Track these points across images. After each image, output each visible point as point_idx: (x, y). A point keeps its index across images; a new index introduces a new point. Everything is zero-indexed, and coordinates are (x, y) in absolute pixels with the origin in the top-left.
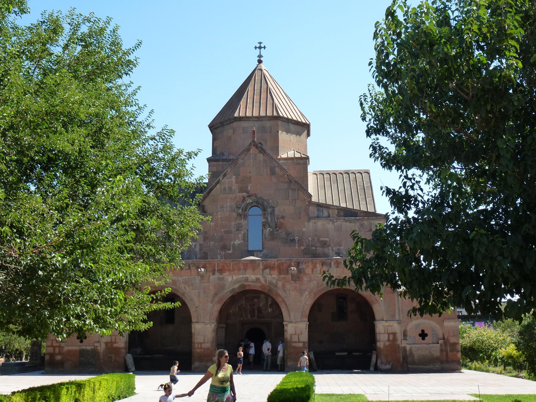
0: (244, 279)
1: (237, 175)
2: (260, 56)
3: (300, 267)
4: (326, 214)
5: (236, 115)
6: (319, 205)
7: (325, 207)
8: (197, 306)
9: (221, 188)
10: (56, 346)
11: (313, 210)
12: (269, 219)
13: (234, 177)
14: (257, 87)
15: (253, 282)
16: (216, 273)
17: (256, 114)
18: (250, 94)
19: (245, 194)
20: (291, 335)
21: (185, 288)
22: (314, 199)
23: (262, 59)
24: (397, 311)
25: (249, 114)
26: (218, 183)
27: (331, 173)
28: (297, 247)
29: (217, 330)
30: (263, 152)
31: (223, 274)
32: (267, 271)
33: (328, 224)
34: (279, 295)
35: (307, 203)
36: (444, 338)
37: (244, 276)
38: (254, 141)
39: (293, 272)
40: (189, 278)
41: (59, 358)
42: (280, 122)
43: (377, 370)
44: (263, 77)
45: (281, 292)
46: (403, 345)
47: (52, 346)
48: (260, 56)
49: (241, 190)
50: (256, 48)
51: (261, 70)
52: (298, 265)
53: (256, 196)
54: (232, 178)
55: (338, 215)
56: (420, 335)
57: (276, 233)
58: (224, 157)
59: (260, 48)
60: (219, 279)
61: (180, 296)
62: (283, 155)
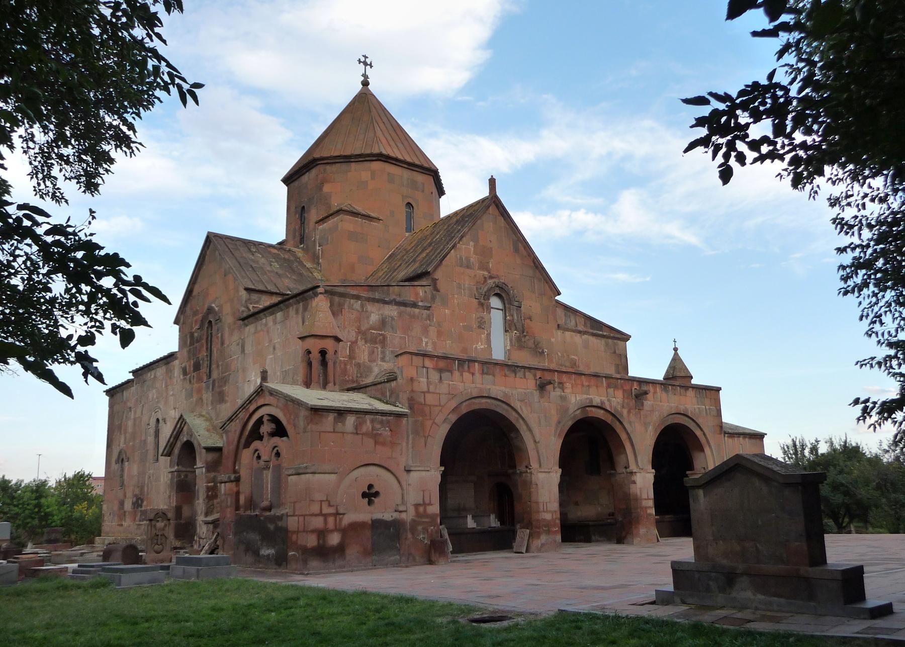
0: (588, 401)
1: (476, 240)
2: (365, 76)
4: (573, 323)
9: (457, 257)
10: (330, 515)
13: (472, 243)
16: (557, 389)
19: (486, 273)
30: (505, 215)
32: (611, 391)
37: (588, 396)
40: (525, 393)
41: (334, 539)
47: (321, 514)
48: (365, 76)
50: (360, 62)
53: (497, 277)
54: (469, 244)
60: (561, 397)
61: (514, 422)
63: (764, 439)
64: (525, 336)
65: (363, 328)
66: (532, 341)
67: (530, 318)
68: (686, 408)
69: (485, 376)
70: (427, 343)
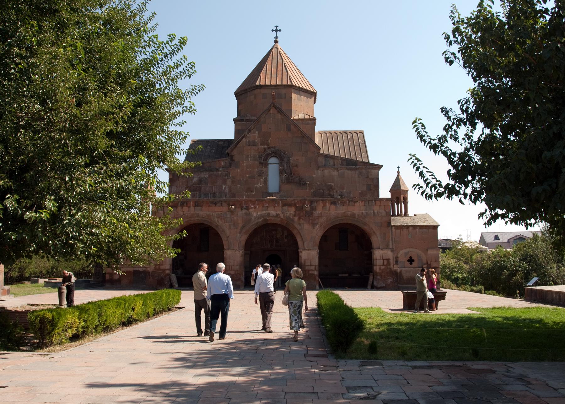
0: (266, 214)
2: (276, 37)
3: (312, 205)
4: (331, 163)
5: (257, 83)
6: (327, 157)
7: (331, 158)
8: (228, 236)
11: (321, 160)
12: (286, 167)
13: (257, 132)
14: (274, 61)
15: (274, 217)
17: (273, 83)
18: (269, 67)
19: (266, 146)
20: (305, 260)
21: (218, 221)
22: (321, 152)
23: (278, 40)
24: (391, 242)
25: (268, 83)
26: (243, 137)
27: (333, 133)
28: (308, 190)
29: (245, 255)
31: (249, 210)
32: (286, 208)
33: (333, 171)
34: (296, 228)
35: (316, 154)
36: (427, 263)
38: (273, 103)
39: (307, 209)
42: (293, 90)
43: (374, 288)
44: (279, 54)
45: (296, 226)
46: (394, 269)
48: (276, 37)
49: (262, 144)
50: (273, 31)
51: (278, 49)
52: (311, 202)
55: (342, 164)
56: (408, 261)
57: (291, 178)
58: (247, 118)
59: (276, 31)
60: (246, 214)
62: (295, 117)
63: (438, 229)
64: (292, 176)
65: (189, 185)
66: (298, 179)
67: (297, 166)
68: (353, 213)
69: (196, 207)
70: (225, 188)
